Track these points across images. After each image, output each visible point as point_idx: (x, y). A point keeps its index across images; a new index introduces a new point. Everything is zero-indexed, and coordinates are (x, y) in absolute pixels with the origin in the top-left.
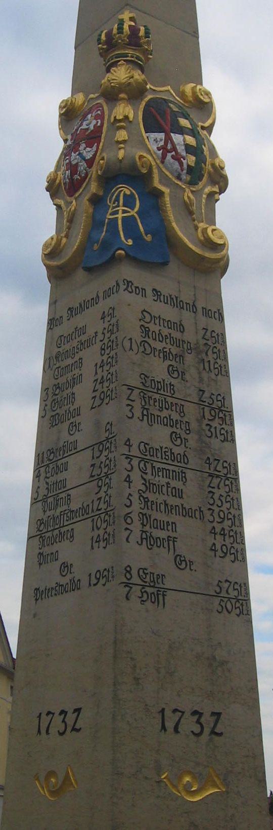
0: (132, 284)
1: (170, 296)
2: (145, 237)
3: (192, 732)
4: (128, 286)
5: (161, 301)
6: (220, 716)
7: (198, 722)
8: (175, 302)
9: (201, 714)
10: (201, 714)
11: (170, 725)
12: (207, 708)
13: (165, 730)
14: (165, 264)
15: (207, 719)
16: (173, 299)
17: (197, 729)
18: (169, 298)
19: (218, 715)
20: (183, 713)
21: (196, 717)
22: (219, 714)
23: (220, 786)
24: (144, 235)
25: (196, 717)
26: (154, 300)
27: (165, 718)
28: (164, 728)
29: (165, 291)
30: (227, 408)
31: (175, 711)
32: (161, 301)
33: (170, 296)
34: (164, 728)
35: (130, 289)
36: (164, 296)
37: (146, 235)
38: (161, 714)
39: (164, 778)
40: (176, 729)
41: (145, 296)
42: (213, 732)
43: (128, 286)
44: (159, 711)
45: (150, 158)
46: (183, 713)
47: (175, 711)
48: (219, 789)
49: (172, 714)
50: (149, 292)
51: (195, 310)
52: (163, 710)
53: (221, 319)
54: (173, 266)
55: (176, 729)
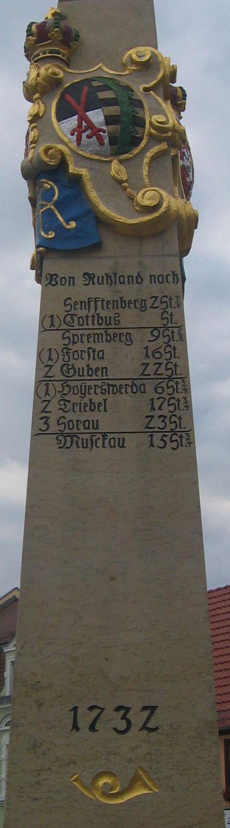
0: (57, 276)
1: (107, 275)
2: (68, 227)
3: (115, 729)
4: (51, 280)
5: (94, 283)
6: (155, 710)
7: (124, 717)
8: (111, 279)
9: (128, 710)
10: (128, 710)
11: (84, 723)
12: (134, 702)
13: (78, 729)
14: (97, 246)
15: (138, 718)
16: (110, 277)
17: (122, 725)
18: (105, 278)
19: (153, 709)
20: (103, 709)
21: (122, 712)
22: (153, 709)
23: (152, 788)
24: (64, 224)
25: (122, 712)
26: (85, 284)
27: (78, 716)
28: (75, 727)
29: (100, 272)
30: (180, 374)
31: (91, 708)
32: (94, 283)
33: (107, 275)
34: (75, 727)
35: (54, 283)
36: (98, 277)
37: (67, 222)
38: (73, 712)
39: (74, 781)
40: (92, 728)
41: (74, 284)
42: (144, 727)
43: (51, 280)
44: (71, 709)
45: (60, 147)
46: (103, 709)
47: (91, 708)
48: (151, 790)
49: (88, 711)
50: (80, 280)
51: (139, 281)
52: (75, 709)
53: (176, 281)
54: (111, 244)
55: (92, 728)
